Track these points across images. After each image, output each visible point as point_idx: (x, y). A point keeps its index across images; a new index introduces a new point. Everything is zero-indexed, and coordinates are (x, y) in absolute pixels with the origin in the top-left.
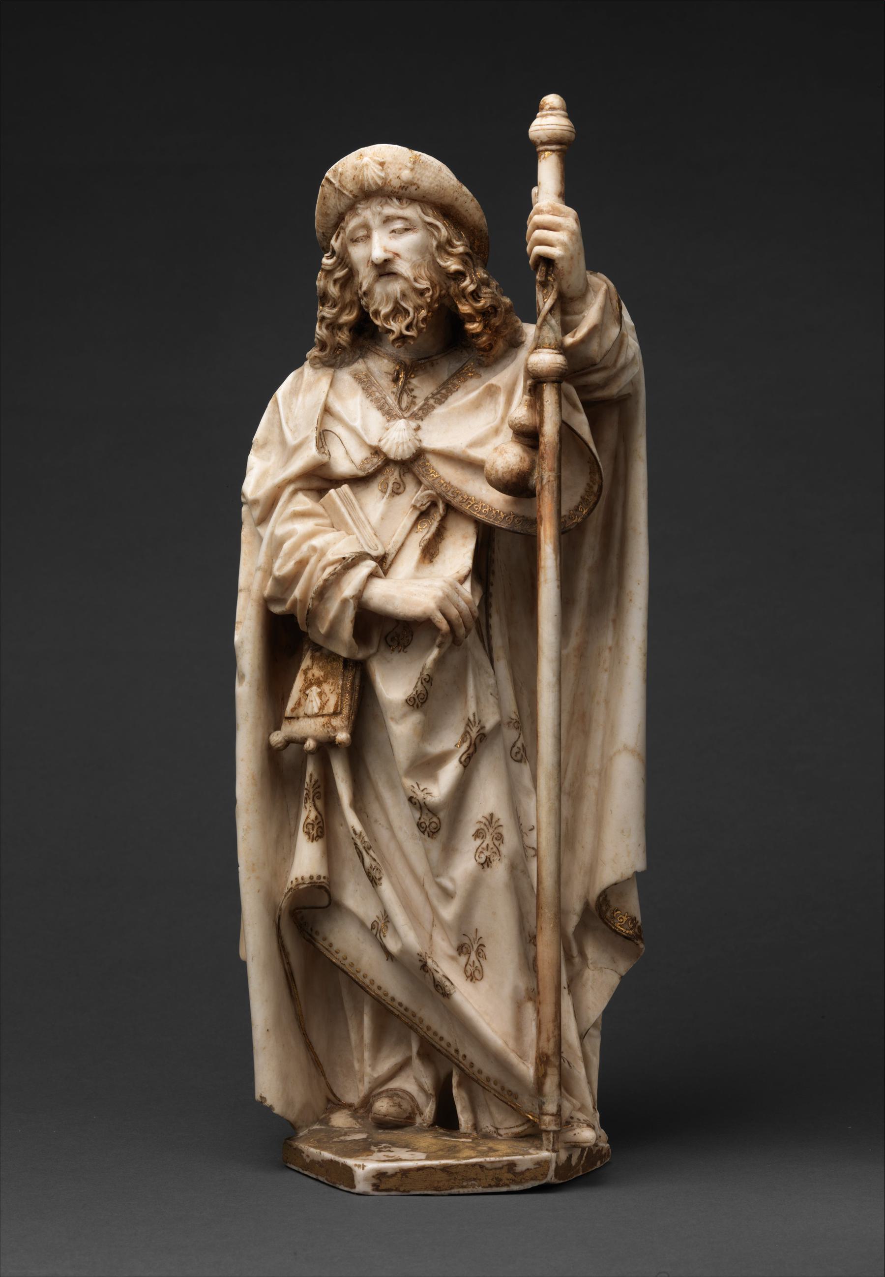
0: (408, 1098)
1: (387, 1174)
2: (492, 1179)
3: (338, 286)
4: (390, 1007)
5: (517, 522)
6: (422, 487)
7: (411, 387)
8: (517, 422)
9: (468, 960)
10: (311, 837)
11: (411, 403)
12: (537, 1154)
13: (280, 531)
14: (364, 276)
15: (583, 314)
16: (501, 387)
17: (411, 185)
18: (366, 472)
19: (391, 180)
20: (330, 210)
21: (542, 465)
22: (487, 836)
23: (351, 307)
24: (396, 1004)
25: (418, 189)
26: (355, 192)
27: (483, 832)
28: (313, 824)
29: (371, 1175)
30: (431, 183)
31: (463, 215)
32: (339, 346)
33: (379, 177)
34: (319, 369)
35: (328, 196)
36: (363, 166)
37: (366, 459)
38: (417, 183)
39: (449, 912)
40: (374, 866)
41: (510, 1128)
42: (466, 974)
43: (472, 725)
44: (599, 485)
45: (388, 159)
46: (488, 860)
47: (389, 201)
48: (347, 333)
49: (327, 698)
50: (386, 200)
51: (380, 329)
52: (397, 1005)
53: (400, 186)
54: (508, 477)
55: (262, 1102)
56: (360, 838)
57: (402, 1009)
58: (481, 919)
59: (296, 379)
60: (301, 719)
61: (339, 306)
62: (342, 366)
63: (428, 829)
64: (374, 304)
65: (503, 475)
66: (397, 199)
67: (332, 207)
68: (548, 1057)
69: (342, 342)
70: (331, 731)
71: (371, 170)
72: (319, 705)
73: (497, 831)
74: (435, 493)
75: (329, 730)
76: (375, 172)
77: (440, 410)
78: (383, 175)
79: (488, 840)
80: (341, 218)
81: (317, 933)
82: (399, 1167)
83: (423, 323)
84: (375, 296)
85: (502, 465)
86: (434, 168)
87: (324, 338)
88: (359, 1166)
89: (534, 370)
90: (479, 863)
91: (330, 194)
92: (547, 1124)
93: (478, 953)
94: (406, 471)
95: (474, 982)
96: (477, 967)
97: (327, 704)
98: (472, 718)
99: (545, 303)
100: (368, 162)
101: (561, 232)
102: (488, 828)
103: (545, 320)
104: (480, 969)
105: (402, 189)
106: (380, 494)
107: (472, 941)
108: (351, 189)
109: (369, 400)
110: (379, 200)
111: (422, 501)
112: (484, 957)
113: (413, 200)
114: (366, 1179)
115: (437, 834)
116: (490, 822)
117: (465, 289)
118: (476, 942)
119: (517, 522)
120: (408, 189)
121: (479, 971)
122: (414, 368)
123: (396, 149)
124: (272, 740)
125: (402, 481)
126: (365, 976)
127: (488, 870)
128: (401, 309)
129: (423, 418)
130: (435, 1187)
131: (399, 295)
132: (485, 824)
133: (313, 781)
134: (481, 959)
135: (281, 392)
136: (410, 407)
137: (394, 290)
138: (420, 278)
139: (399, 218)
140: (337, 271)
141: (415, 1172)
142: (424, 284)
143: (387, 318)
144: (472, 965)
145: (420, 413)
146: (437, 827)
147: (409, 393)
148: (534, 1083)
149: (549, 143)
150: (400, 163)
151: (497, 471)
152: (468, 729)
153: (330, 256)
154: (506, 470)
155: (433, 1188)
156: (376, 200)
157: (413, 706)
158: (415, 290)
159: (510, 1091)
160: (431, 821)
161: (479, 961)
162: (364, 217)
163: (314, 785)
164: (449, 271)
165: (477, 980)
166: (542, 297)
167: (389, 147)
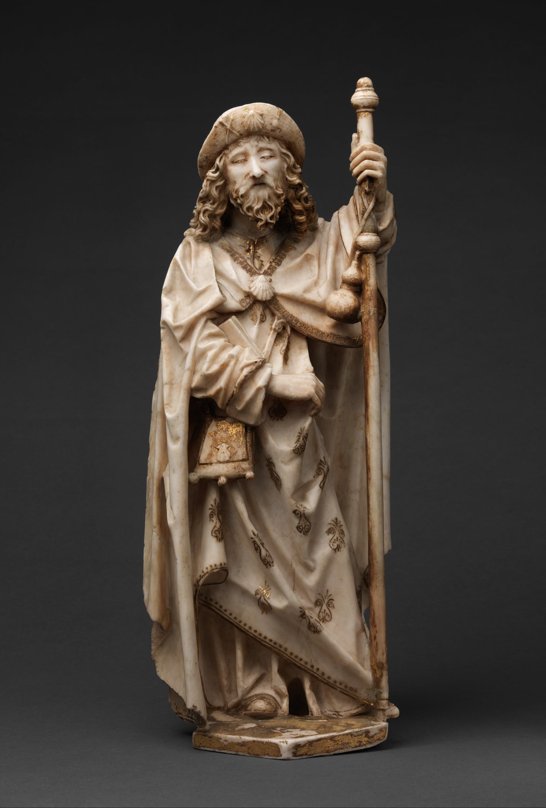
0: (272, 699)
1: (301, 745)
2: (357, 742)
3: (218, 190)
4: (263, 643)
5: (336, 339)
6: (276, 318)
7: (258, 255)
8: (352, 277)
9: (321, 610)
10: (219, 539)
12: (379, 724)
13: (202, 346)
14: (241, 184)
15: (384, 212)
16: (314, 255)
18: (245, 308)
19: (266, 125)
20: (219, 143)
21: (369, 304)
22: (336, 532)
23: (223, 204)
24: (267, 641)
25: (281, 132)
26: (242, 132)
27: (333, 529)
28: (219, 531)
29: (292, 747)
30: (287, 129)
32: (214, 229)
33: (261, 123)
34: (200, 243)
35: (219, 133)
36: (250, 116)
37: (242, 299)
39: (311, 580)
40: (268, 555)
41: (348, 710)
42: (319, 618)
43: (324, 464)
44: (383, 317)
45: (265, 112)
46: (338, 546)
47: (262, 138)
48: (219, 221)
49: (235, 451)
50: (260, 138)
52: (268, 641)
53: (271, 130)
54: (347, 311)
55: (194, 709)
56: (258, 538)
57: (272, 643)
58: (332, 584)
59: (184, 249)
60: (213, 465)
61: (217, 203)
62: (213, 241)
63: (304, 530)
64: (248, 203)
65: (345, 310)
66: (267, 137)
67: (221, 141)
68: (383, 664)
69: (217, 227)
70: (241, 471)
71: (256, 119)
72: (229, 455)
73: (340, 529)
74: (285, 321)
75: (240, 470)
77: (279, 270)
78: (263, 122)
79: (337, 535)
80: (226, 147)
81: (211, 600)
82: (307, 740)
84: (250, 198)
85: (344, 303)
87: (207, 223)
88: (283, 742)
89: (365, 245)
90: (333, 549)
91: (221, 133)
92: (384, 706)
93: (328, 605)
94: (266, 307)
95: (325, 623)
96: (327, 613)
97: (236, 454)
98: (323, 460)
99: (369, 205)
101: (380, 162)
102: (336, 527)
103: (369, 215)
104: (329, 614)
105: (272, 131)
106: (252, 322)
107: (324, 597)
108: (239, 130)
109: (236, 263)
110: (256, 137)
111: (279, 326)
112: (333, 606)
114: (289, 750)
115: (308, 533)
116: (337, 524)
118: (327, 598)
119: (336, 339)
120: (275, 131)
121: (329, 616)
124: (191, 479)
125: (264, 314)
126: (245, 625)
127: (338, 553)
128: (267, 206)
129: (271, 274)
130: (327, 751)
131: (267, 197)
132: (334, 525)
133: (217, 503)
134: (330, 608)
135: (178, 256)
137: (264, 194)
139: (268, 149)
140: (219, 181)
141: (316, 742)
142: (280, 191)
143: (258, 211)
144: (323, 612)
145: (269, 271)
146: (309, 528)
148: (373, 682)
149: (364, 107)
150: (272, 115)
151: (341, 308)
152: (321, 467)
153: (215, 171)
154: (347, 306)
155: (325, 751)
156: (254, 138)
157: (297, 453)
159: (351, 688)
160: (306, 524)
161: (329, 609)
162: (246, 148)
163: (218, 506)
164: (295, 183)
165: (327, 621)
166: (366, 201)
167: (264, 104)
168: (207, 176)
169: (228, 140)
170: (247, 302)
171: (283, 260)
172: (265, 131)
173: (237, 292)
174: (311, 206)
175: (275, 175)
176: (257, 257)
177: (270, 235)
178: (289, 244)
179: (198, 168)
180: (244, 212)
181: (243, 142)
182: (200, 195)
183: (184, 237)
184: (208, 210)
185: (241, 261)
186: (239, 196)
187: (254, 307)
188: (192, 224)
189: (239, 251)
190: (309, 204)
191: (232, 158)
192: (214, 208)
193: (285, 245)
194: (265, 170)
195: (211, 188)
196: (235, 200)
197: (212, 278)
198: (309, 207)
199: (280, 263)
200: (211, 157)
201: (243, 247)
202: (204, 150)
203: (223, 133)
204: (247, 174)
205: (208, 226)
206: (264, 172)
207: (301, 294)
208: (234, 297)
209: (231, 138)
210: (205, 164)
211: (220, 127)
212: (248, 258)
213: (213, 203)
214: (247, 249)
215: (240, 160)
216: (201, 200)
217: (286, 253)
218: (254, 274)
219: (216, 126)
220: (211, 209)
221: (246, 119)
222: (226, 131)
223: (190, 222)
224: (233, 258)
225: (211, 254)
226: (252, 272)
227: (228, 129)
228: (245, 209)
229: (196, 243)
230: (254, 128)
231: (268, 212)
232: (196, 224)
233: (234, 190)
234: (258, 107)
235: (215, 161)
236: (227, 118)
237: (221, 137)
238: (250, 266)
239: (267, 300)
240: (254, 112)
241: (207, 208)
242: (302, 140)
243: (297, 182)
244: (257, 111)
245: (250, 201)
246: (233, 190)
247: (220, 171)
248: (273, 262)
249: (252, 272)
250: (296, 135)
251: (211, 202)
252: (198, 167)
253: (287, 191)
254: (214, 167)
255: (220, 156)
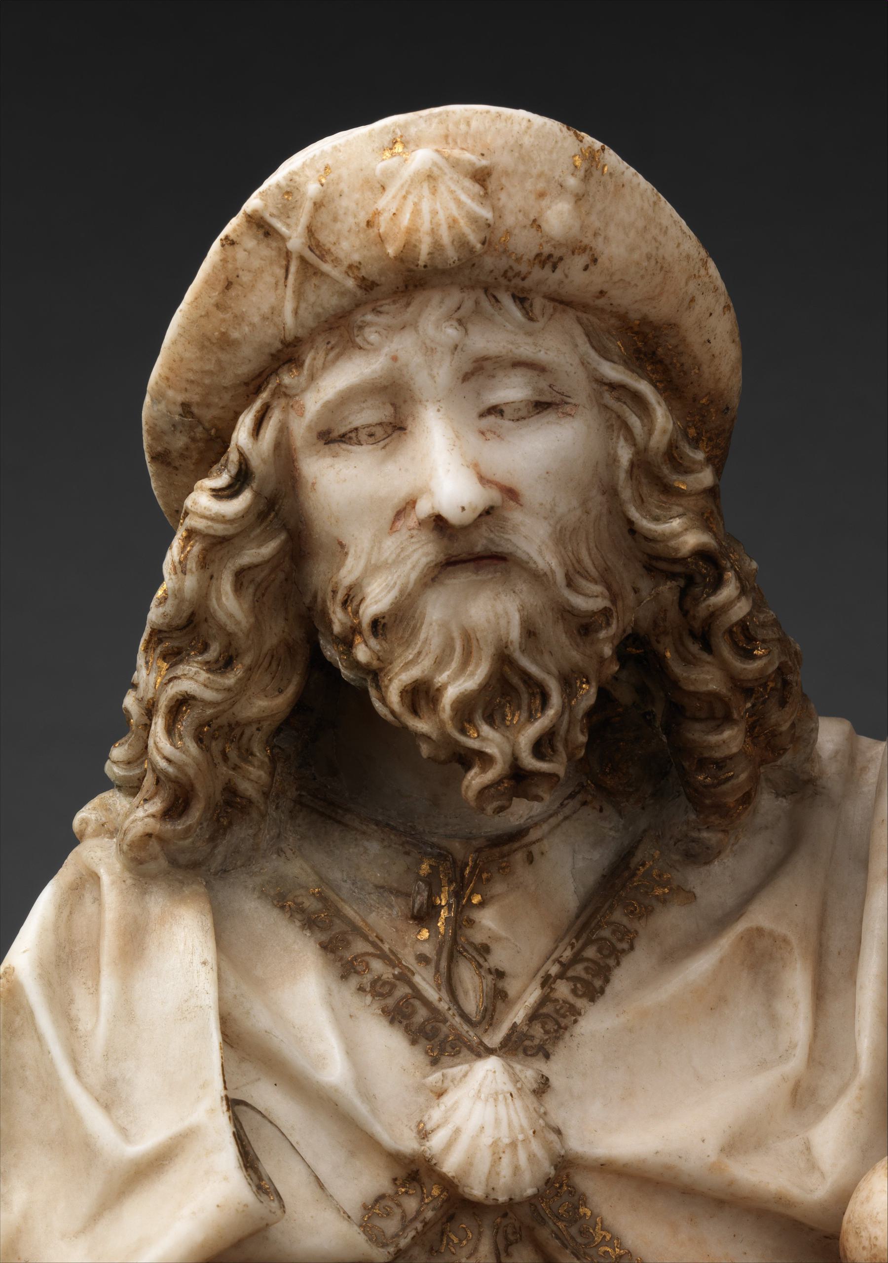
7: (478, 938)
11: (495, 997)
17: (573, 253)
18: (392, 1249)
25: (592, 268)
26: (371, 271)
31: (695, 358)
33: (474, 220)
35: (246, 278)
37: (381, 1198)
38: (593, 245)
45: (504, 160)
47: (486, 304)
51: (425, 750)
53: (538, 255)
59: (66, 913)
61: (248, 660)
66: (514, 297)
67: (256, 319)
69: (247, 788)
76: (459, 203)
78: (486, 213)
83: (582, 732)
84: (422, 636)
86: (642, 195)
87: (191, 772)
100: (435, 169)
105: (543, 264)
108: (356, 257)
110: (454, 297)
113: (562, 302)
117: (715, 614)
122: (481, 872)
123: (525, 124)
128: (516, 680)
131: (515, 633)
136: (494, 1010)
138: (582, 576)
139: (518, 364)
145: (537, 1031)
147: (481, 961)
150: (540, 175)
153: (229, 486)
158: (565, 613)
162: (395, 359)
164: (677, 550)
168: (186, 514)
169: (296, 312)
170: (404, 1211)
171: (618, 964)
172: (504, 263)
173: (352, 1154)
174: (771, 669)
175: (562, 509)
176: (476, 948)
177: (553, 821)
178: (655, 872)
179: (148, 465)
180: (393, 712)
181: (376, 324)
182: (155, 615)
183: (72, 841)
184: (193, 698)
185: (379, 978)
186: (360, 623)
187: (450, 1240)
188: (116, 769)
189: (372, 918)
190: (757, 665)
191: (320, 415)
192: (229, 690)
193: (634, 875)
194: (507, 483)
195: (209, 578)
196: (346, 643)
197: (204, 1086)
198: (762, 680)
199: (598, 983)
200: (208, 406)
201: (398, 893)
202: (171, 369)
203: (268, 278)
204: (404, 504)
205: (198, 787)
206: (493, 496)
207: (713, 1158)
208: (331, 1190)
209: (313, 305)
210: (180, 441)
211: (250, 243)
212: (423, 959)
213: (221, 663)
214: (417, 906)
215: (364, 427)
216: (160, 641)
217: (637, 925)
218: (449, 1049)
219: (227, 238)
220: (209, 695)
221: (394, 197)
222: (284, 263)
223: (106, 757)
224: (335, 961)
225: (211, 944)
226: (442, 1036)
227: (294, 256)
228: (394, 696)
229: (129, 882)
230: (437, 246)
231: (525, 715)
232: (137, 771)
233: (334, 592)
234: (463, 127)
235: (232, 427)
236: (289, 192)
237: (254, 299)
238: (426, 1003)
239: (517, 1198)
240: (436, 157)
241: (185, 686)
242: (719, 309)
243: (686, 542)
244: (456, 153)
245: (419, 653)
246: (330, 589)
247: (254, 485)
248: (561, 976)
249: (442, 1036)
250: (683, 284)
251: (213, 653)
252: (147, 458)
253: (636, 591)
254: (226, 466)
255: (257, 405)
